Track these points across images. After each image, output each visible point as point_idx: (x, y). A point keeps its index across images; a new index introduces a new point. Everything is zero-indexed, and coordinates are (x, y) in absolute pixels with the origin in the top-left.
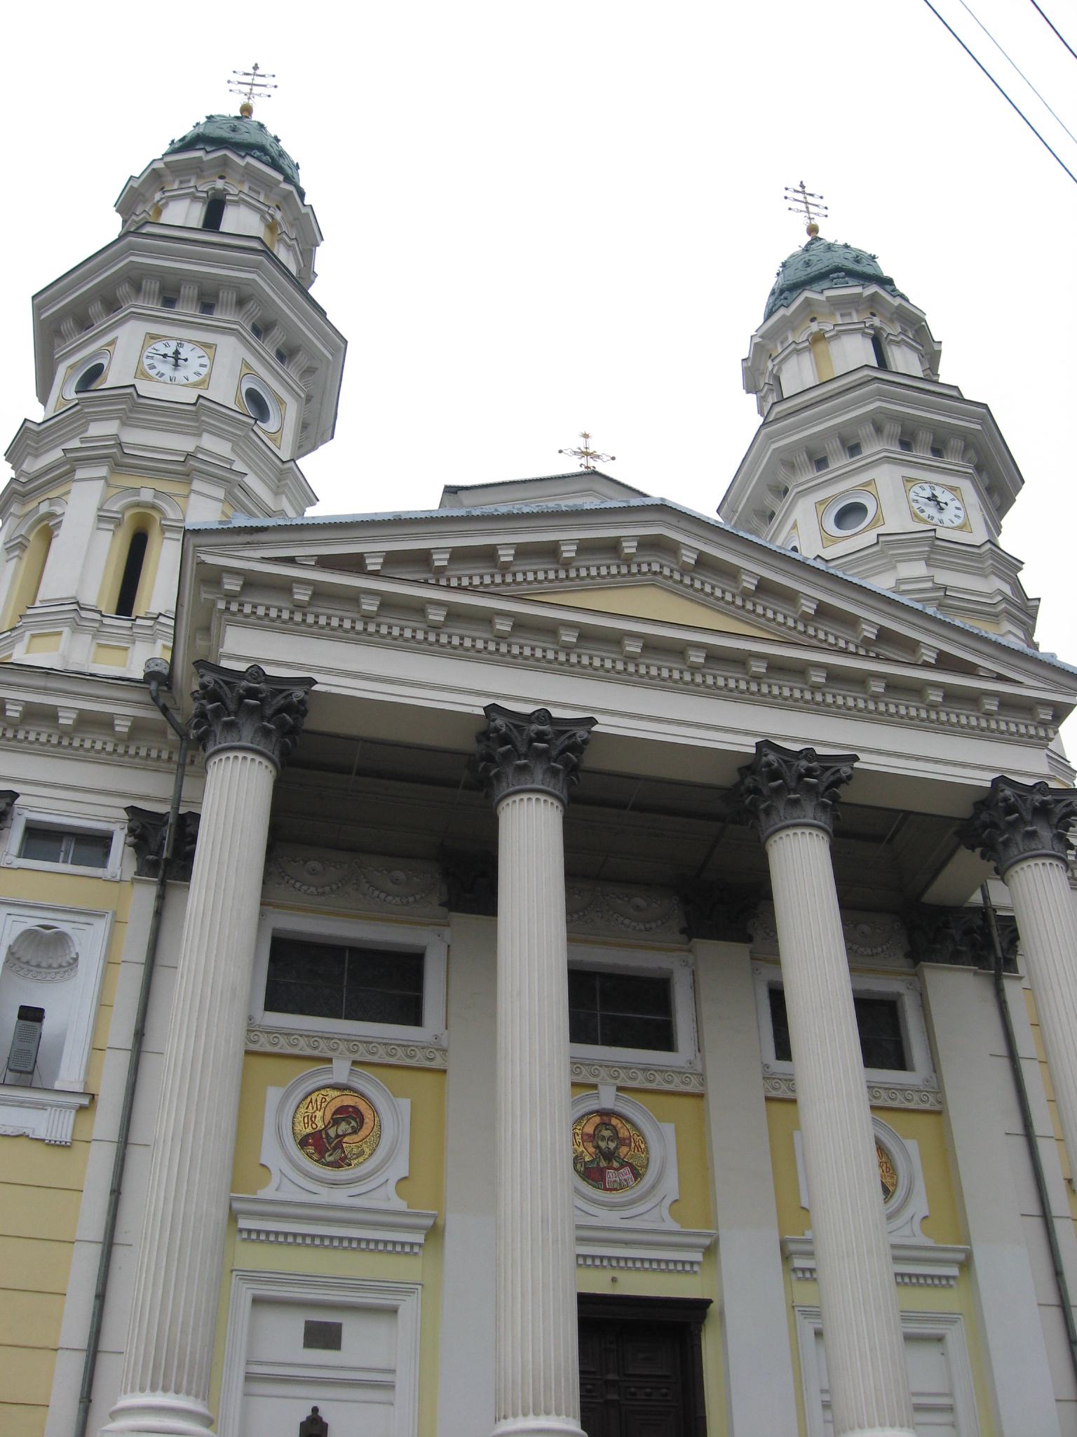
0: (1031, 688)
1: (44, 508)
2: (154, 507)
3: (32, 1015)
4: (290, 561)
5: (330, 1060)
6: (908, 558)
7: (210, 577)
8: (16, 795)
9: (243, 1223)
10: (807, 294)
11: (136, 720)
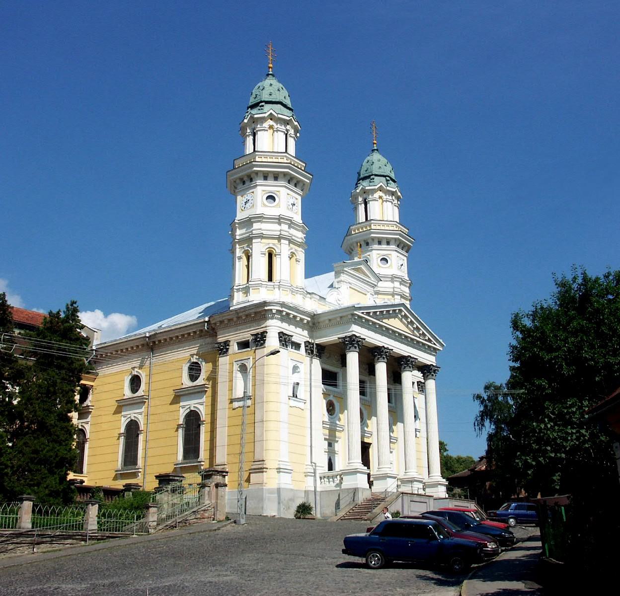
0: (438, 347)
1: (271, 246)
2: (294, 253)
3: (298, 384)
4: (363, 313)
5: (330, 395)
6: (396, 281)
7: (353, 315)
8: (292, 336)
9: (324, 425)
10: (381, 184)
11: (308, 321)
